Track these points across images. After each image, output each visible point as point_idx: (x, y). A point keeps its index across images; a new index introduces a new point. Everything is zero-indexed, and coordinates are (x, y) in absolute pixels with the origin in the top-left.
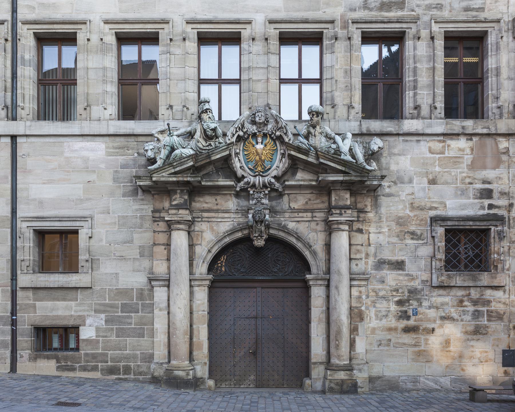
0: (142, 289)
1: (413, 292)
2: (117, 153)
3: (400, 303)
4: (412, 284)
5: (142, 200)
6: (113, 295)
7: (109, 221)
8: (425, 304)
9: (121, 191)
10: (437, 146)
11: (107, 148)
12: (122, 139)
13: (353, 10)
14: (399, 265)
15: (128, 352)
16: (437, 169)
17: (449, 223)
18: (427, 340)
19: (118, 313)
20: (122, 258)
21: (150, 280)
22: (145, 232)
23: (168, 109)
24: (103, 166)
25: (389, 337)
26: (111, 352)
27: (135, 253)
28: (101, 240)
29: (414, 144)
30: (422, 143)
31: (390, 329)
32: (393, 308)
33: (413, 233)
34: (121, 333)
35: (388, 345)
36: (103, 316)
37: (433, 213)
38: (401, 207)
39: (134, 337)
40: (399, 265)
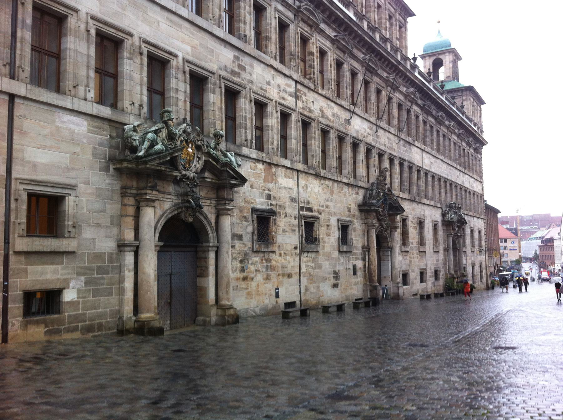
0: (112, 253)
1: (246, 254)
2: (96, 131)
3: (241, 262)
4: (245, 249)
5: (113, 176)
6: (91, 259)
7: (89, 191)
8: (250, 262)
9: (97, 166)
10: (253, 165)
11: (89, 125)
12: (99, 121)
13: (221, 69)
14: (240, 237)
15: (101, 310)
16: (253, 179)
17: (259, 213)
18: (251, 285)
19: (94, 274)
20: (98, 225)
21: (119, 246)
22: (114, 203)
23: (131, 105)
24: (85, 141)
25: (237, 284)
26: (89, 311)
27: (106, 221)
28: (83, 208)
29: (245, 162)
30: (248, 162)
31: (238, 279)
32: (239, 265)
33: (245, 217)
34: (96, 293)
35: (237, 289)
36: (83, 278)
37: (252, 205)
38: (241, 200)
39: (105, 296)
40: (240, 237)
